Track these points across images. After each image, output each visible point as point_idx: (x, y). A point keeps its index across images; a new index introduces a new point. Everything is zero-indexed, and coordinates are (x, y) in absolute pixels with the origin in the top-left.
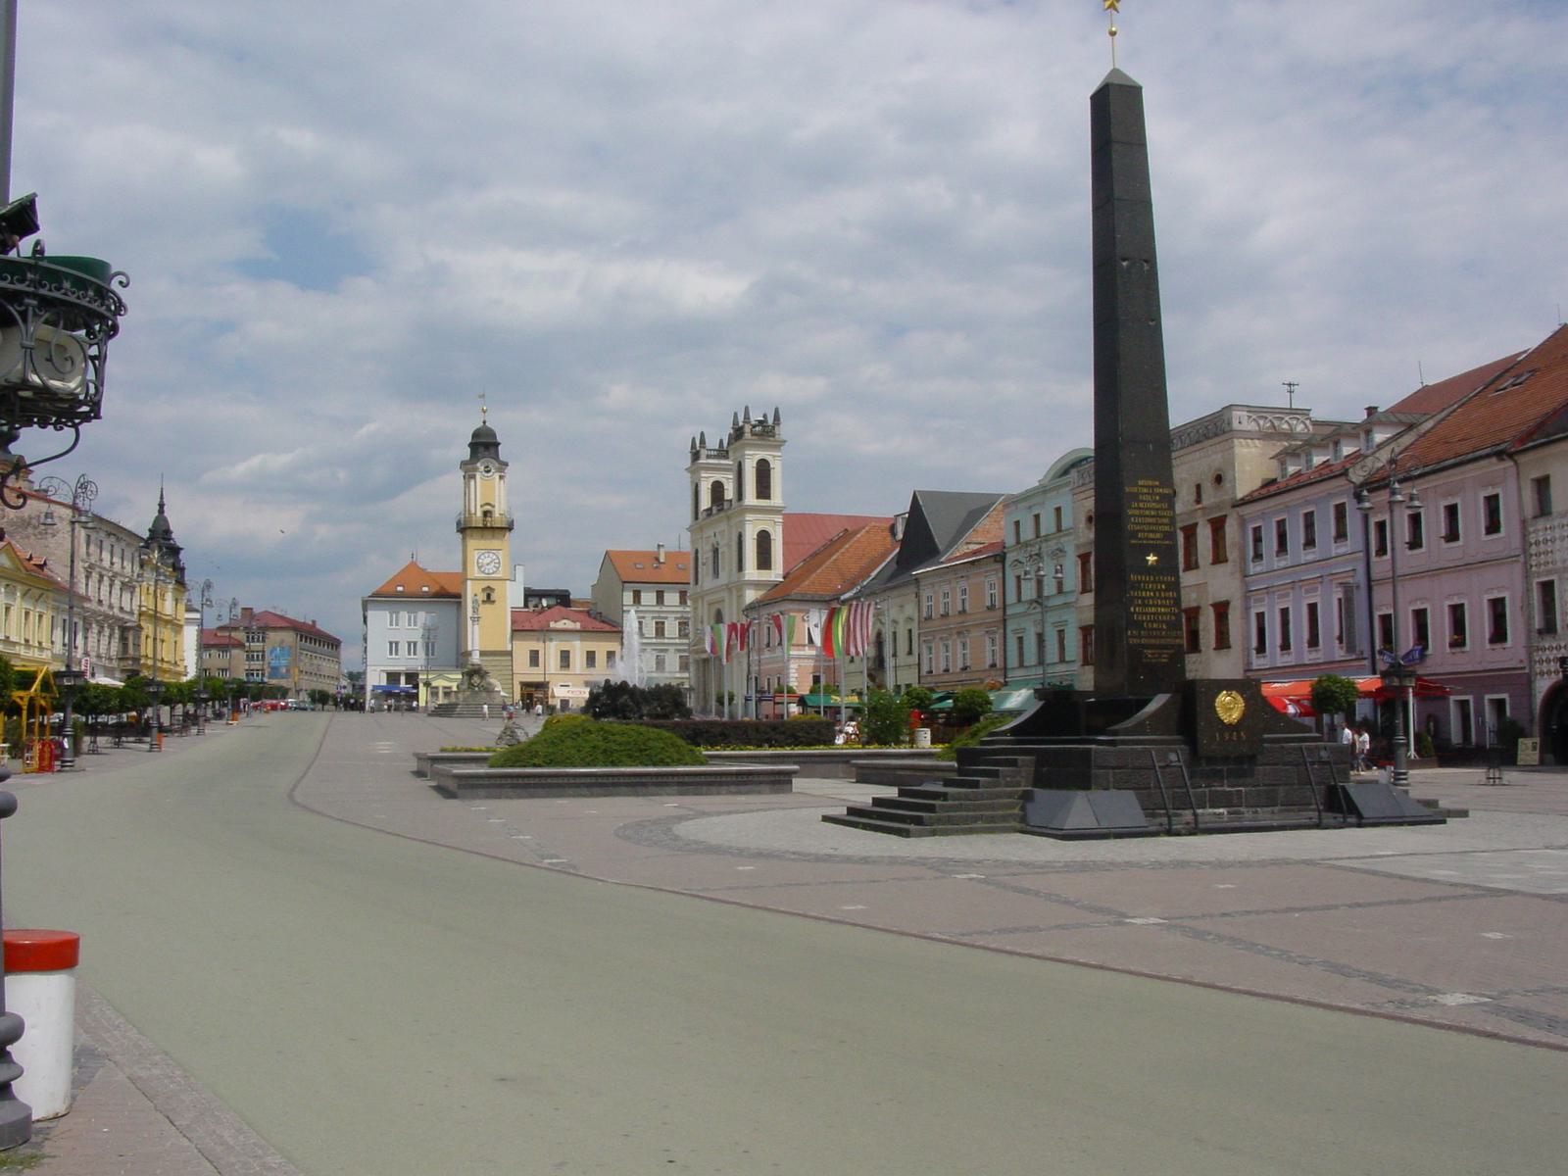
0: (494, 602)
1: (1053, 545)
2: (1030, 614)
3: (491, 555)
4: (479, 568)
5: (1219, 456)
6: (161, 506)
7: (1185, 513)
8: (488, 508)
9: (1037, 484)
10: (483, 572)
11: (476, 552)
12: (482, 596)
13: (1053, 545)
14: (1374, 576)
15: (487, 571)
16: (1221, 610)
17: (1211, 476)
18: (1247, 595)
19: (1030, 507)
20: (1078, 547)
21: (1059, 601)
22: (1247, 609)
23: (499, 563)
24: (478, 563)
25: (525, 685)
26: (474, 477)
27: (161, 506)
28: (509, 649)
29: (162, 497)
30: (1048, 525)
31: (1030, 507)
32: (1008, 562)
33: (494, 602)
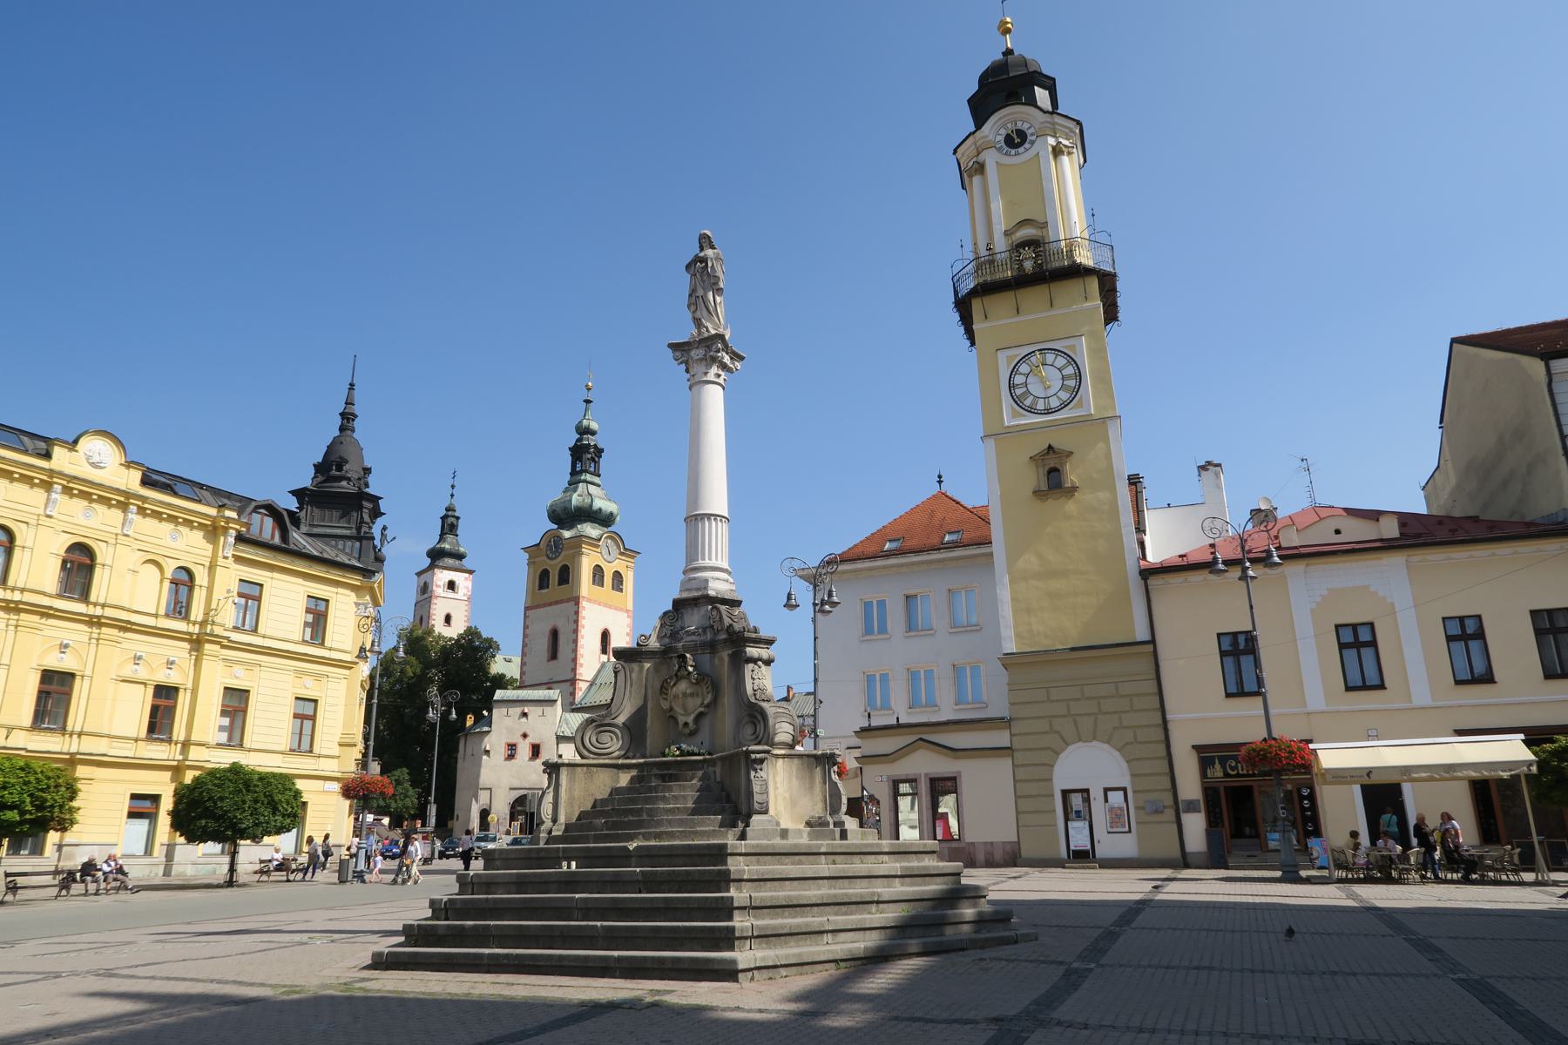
0: (1074, 489)
3: (1050, 357)
4: (1017, 401)
6: (347, 417)
8: (1027, 232)
10: (1031, 410)
11: (1002, 357)
12: (1032, 478)
15: (1041, 406)
23: (1079, 375)
24: (1011, 387)
25: (1207, 755)
26: (980, 168)
27: (347, 417)
28: (1142, 634)
29: (349, 403)
33: (1074, 489)
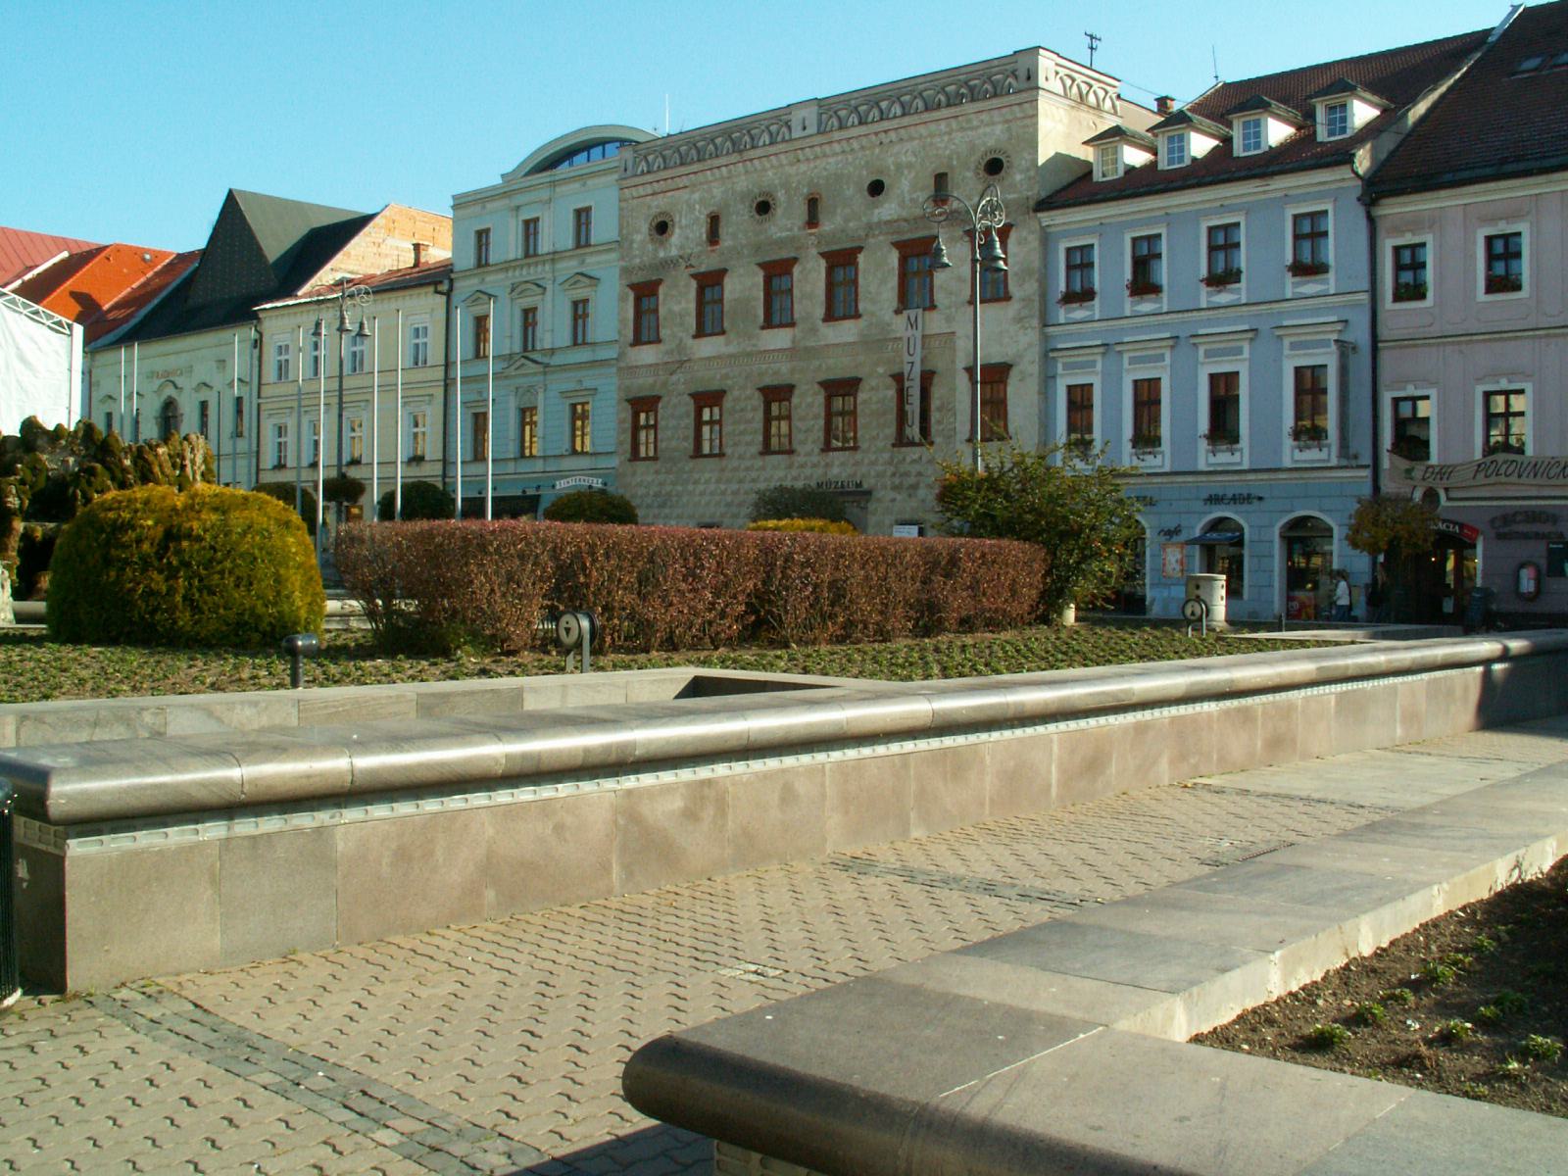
1: (567, 267)
2: (506, 377)
5: (999, 129)
7: (906, 220)
9: (499, 181)
13: (567, 267)
14: (1384, 332)
16: (996, 375)
17: (978, 158)
18: (1048, 354)
19: (518, 208)
20: (626, 271)
21: (582, 355)
22: (1047, 379)
30: (556, 233)
31: (518, 208)
32: (456, 297)
